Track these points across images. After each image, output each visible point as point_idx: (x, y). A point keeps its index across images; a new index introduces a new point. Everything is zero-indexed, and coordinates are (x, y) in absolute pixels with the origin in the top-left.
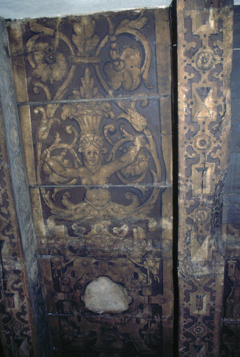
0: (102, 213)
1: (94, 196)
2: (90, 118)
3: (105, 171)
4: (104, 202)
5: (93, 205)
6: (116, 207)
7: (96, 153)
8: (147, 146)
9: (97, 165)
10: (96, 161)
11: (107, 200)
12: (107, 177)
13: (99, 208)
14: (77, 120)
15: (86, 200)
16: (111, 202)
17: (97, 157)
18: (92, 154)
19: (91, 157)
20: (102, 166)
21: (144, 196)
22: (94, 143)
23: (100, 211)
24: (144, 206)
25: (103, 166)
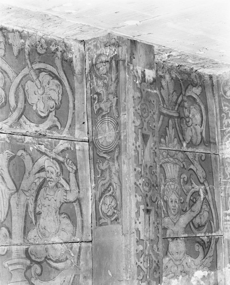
0: (180, 269)
1: (174, 249)
2: (172, 165)
3: (182, 221)
4: (181, 255)
5: (174, 260)
6: (189, 260)
7: (176, 202)
8: (207, 196)
9: (177, 215)
10: (177, 211)
11: (183, 253)
12: (184, 228)
13: (178, 263)
14: (164, 167)
15: (168, 253)
16: (186, 254)
17: (177, 206)
18: (173, 202)
19: (173, 206)
20: (180, 215)
21: (206, 247)
22: (175, 192)
23: (178, 266)
24: (207, 258)
25: (181, 216)
